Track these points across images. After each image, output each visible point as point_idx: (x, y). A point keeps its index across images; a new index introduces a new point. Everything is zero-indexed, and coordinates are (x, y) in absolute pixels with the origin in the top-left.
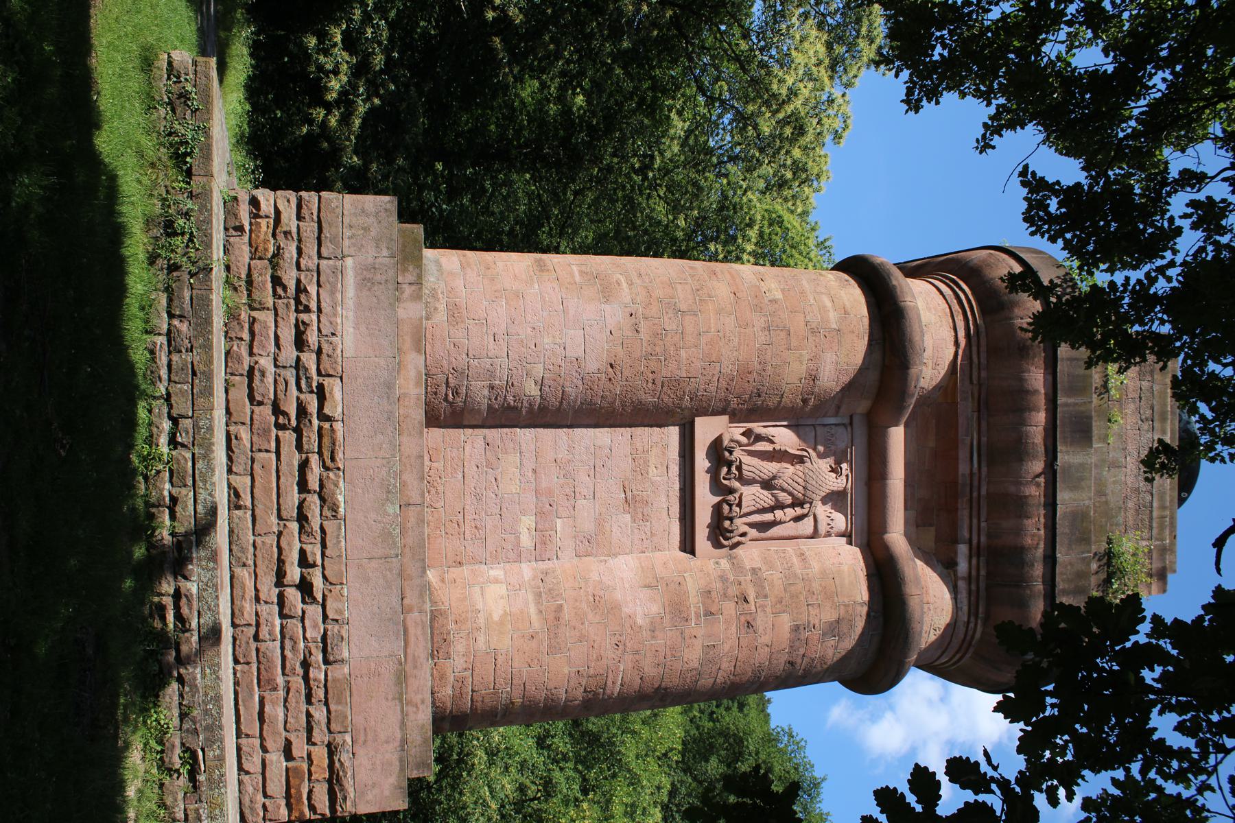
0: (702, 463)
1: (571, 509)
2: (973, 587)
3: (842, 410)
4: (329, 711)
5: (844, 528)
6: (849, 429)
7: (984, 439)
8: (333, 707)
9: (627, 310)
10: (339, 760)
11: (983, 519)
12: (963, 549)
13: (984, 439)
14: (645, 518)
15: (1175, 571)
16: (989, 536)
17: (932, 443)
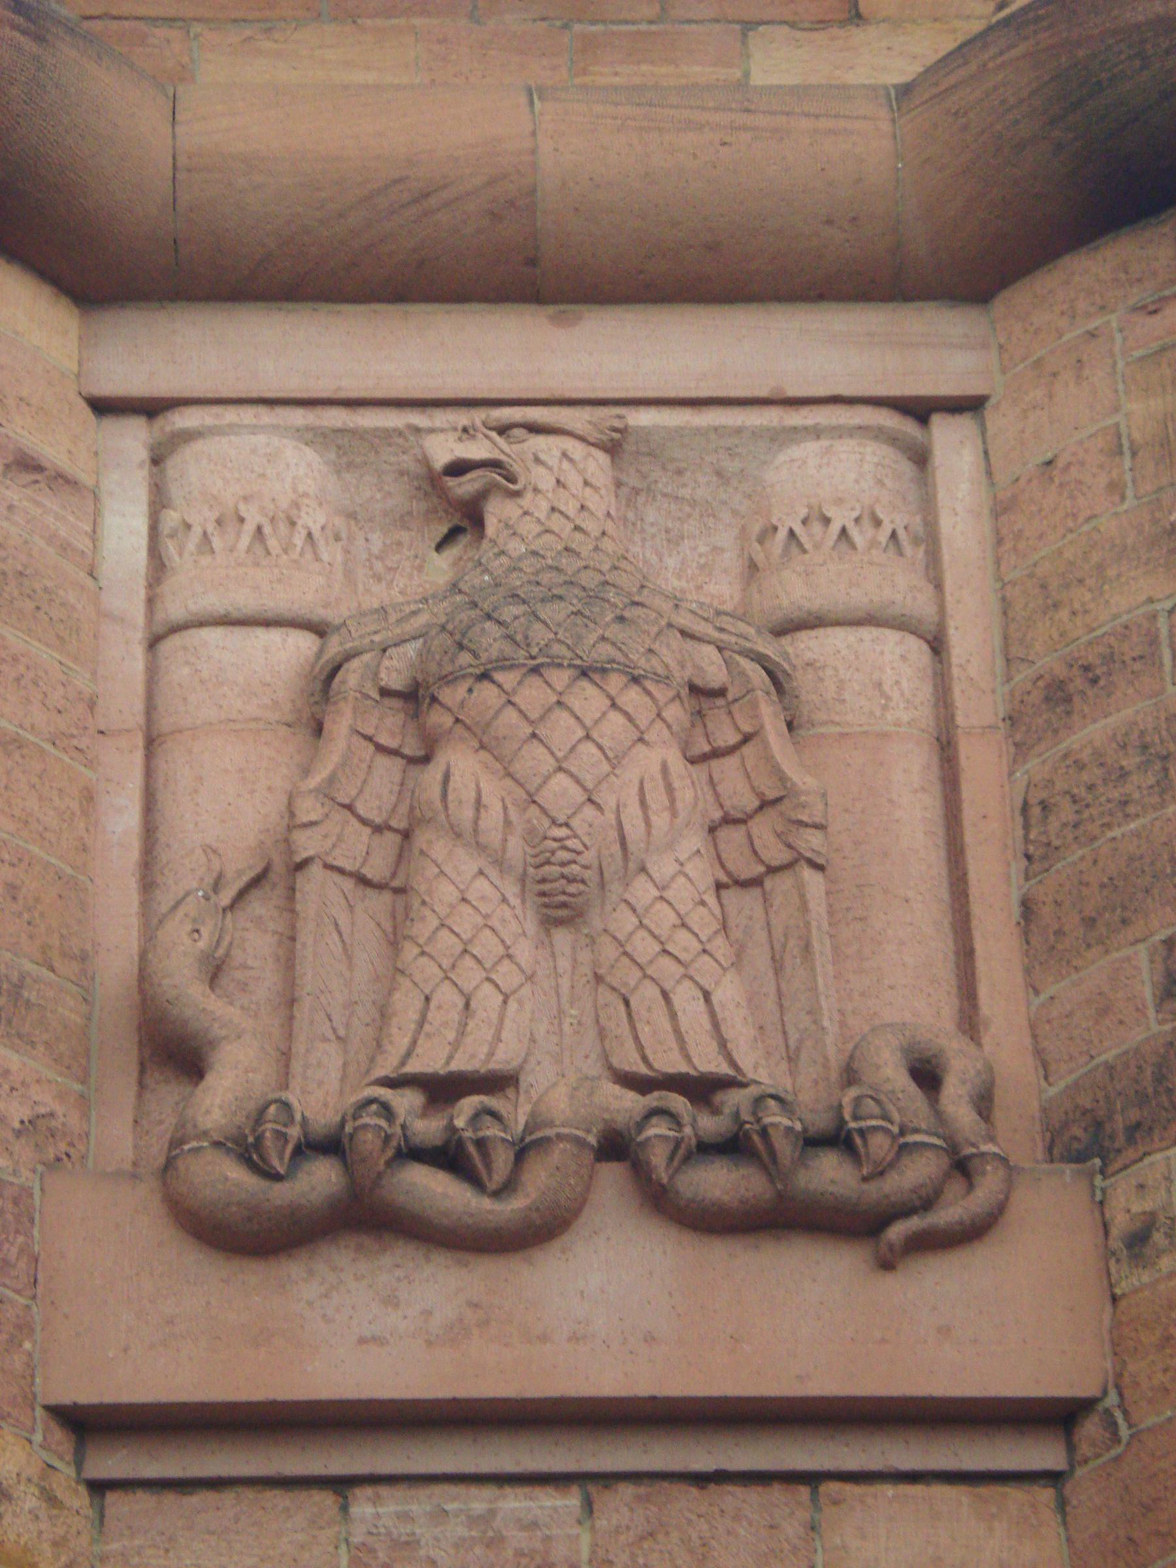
5: (875, 453)
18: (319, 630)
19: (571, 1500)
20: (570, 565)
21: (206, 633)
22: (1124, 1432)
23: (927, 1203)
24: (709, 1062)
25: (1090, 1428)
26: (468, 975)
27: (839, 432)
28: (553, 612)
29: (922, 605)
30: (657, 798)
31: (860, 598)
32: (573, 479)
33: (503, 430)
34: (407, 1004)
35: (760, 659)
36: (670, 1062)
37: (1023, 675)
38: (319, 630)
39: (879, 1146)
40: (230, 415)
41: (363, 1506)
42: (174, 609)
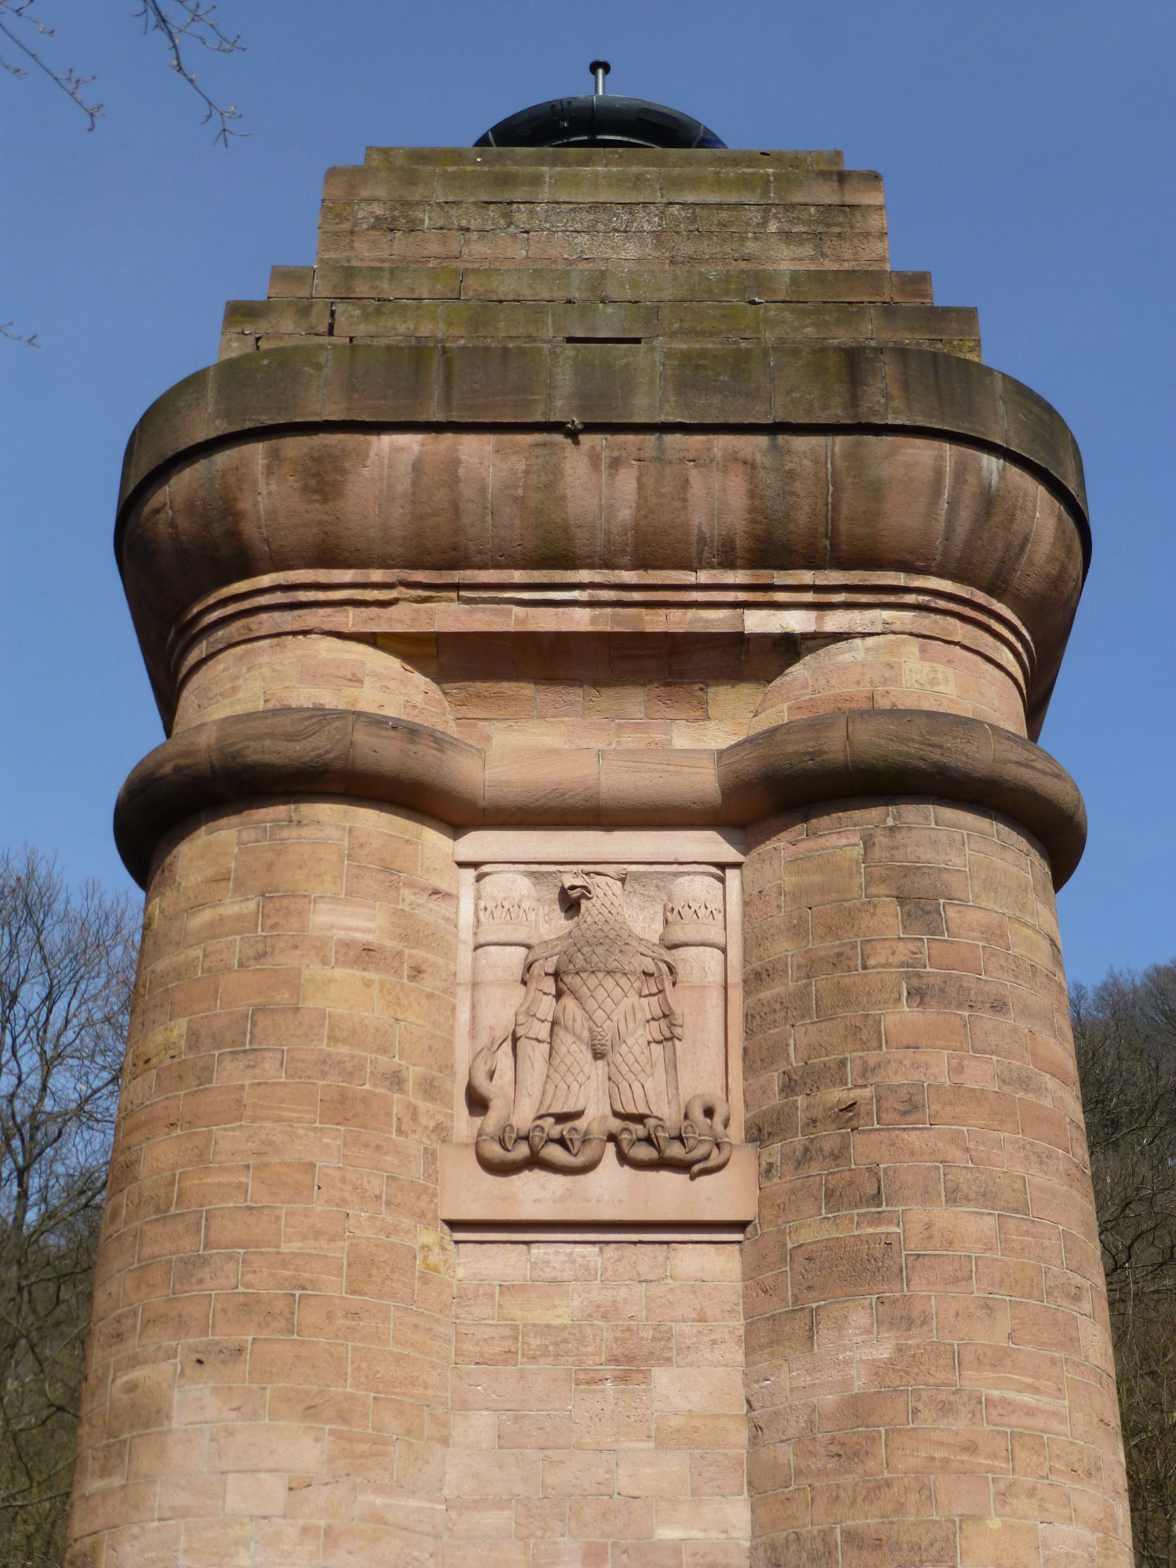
1: (635, 1503)
3: (444, 886)
6: (485, 869)
7: (518, 576)
9: (188, 1371)
11: (690, 578)
12: (757, 622)
14: (664, 1336)
15: (838, 154)
16: (729, 564)
17: (527, 690)
18: (528, 947)
20: (606, 928)
21: (491, 948)
22: (759, 1232)
23: (706, 1158)
24: (642, 1110)
25: (750, 1229)
26: (570, 1078)
27: (695, 873)
28: (600, 950)
29: (719, 939)
30: (630, 1018)
31: (699, 938)
32: (609, 893)
33: (587, 874)
34: (550, 1088)
35: (666, 962)
36: (631, 1109)
37: (749, 967)
38: (528, 947)
39: (691, 1143)
40: (501, 867)
41: (535, 1249)
42: (482, 940)
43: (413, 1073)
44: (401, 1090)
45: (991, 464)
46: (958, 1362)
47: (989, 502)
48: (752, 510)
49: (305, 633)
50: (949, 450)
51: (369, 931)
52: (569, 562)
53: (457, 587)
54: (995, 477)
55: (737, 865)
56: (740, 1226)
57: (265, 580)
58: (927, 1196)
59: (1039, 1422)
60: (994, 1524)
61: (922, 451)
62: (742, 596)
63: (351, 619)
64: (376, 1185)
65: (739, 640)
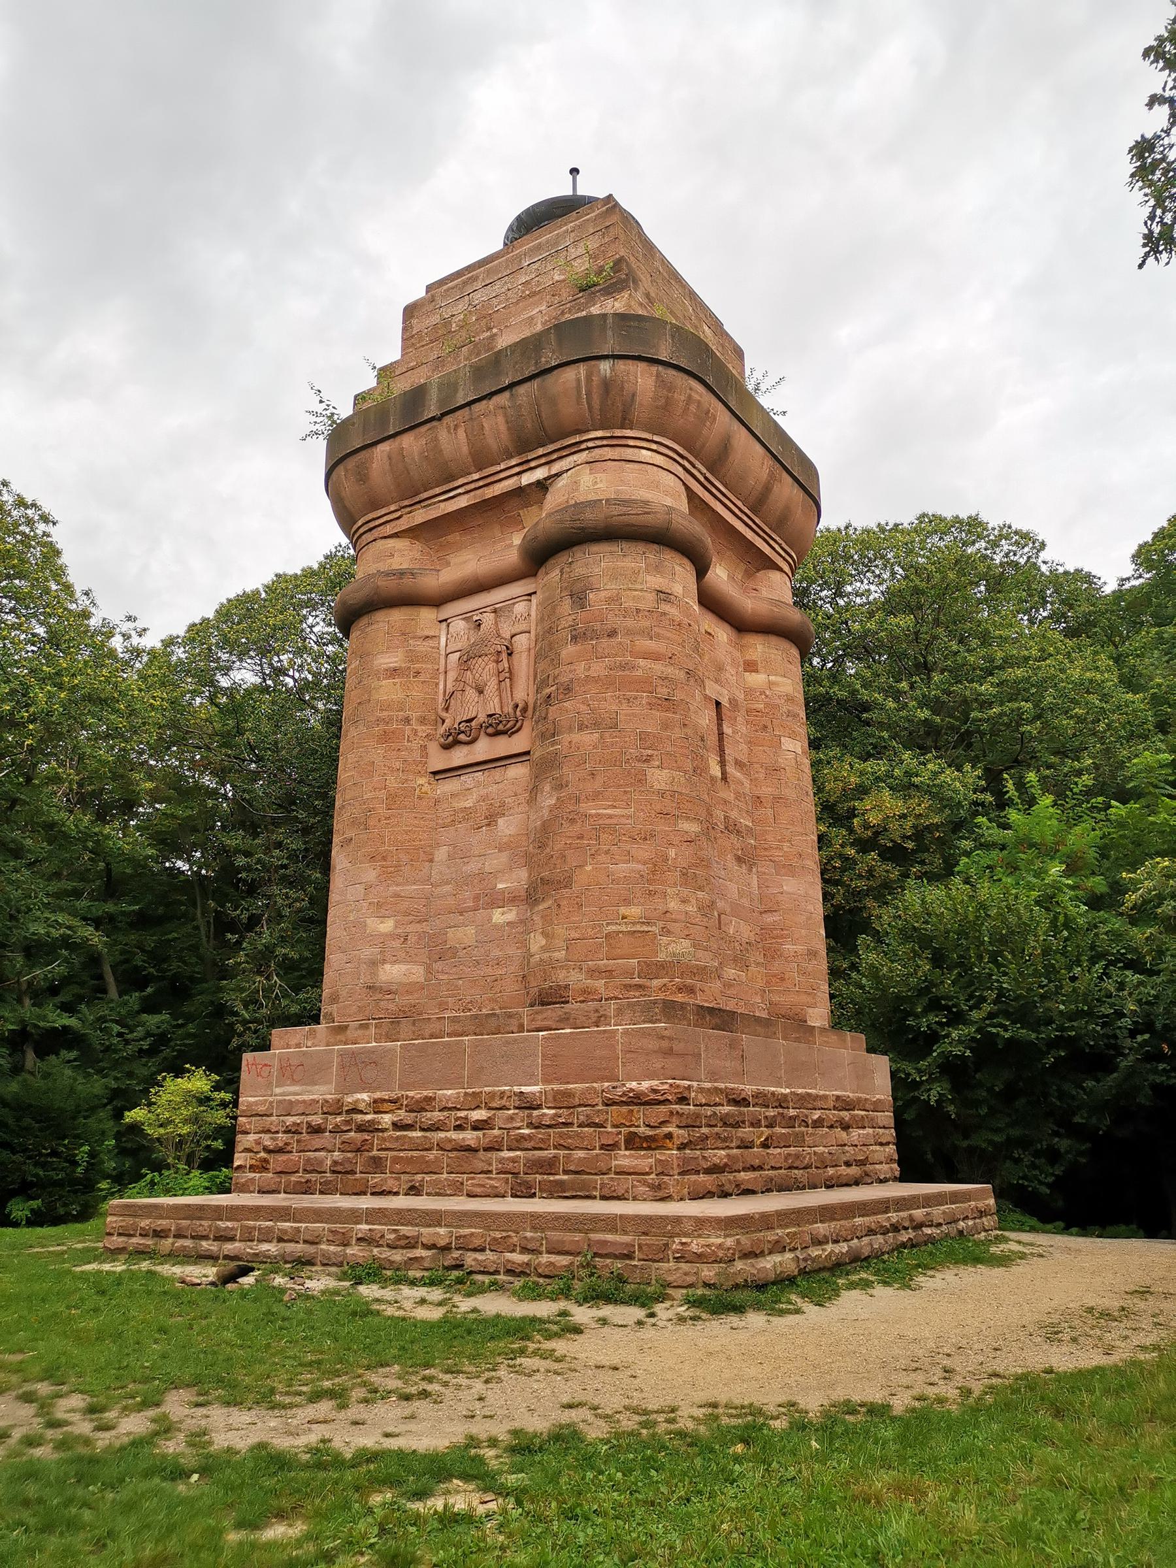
0: (459, 756)
2: (555, 456)
4: (580, 1105)
7: (438, 490)
8: (577, 1101)
10: (620, 1096)
11: (498, 468)
12: (527, 479)
13: (438, 490)
14: (503, 804)
16: (510, 457)
19: (481, 773)
43: (414, 715)
44: (409, 725)
45: (605, 367)
46: (578, 800)
47: (607, 385)
48: (509, 429)
49: (374, 540)
50: (582, 369)
51: (396, 662)
52: (454, 478)
53: (420, 502)
54: (608, 371)
55: (535, 593)
56: (527, 753)
57: (360, 523)
58: (570, 729)
59: (614, 821)
60: (589, 868)
61: (569, 375)
62: (517, 469)
63: (389, 529)
64: (398, 765)
65: (519, 491)
